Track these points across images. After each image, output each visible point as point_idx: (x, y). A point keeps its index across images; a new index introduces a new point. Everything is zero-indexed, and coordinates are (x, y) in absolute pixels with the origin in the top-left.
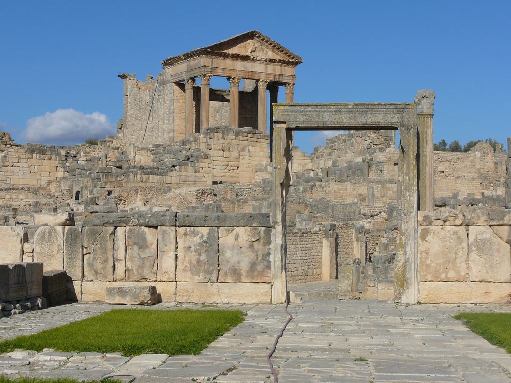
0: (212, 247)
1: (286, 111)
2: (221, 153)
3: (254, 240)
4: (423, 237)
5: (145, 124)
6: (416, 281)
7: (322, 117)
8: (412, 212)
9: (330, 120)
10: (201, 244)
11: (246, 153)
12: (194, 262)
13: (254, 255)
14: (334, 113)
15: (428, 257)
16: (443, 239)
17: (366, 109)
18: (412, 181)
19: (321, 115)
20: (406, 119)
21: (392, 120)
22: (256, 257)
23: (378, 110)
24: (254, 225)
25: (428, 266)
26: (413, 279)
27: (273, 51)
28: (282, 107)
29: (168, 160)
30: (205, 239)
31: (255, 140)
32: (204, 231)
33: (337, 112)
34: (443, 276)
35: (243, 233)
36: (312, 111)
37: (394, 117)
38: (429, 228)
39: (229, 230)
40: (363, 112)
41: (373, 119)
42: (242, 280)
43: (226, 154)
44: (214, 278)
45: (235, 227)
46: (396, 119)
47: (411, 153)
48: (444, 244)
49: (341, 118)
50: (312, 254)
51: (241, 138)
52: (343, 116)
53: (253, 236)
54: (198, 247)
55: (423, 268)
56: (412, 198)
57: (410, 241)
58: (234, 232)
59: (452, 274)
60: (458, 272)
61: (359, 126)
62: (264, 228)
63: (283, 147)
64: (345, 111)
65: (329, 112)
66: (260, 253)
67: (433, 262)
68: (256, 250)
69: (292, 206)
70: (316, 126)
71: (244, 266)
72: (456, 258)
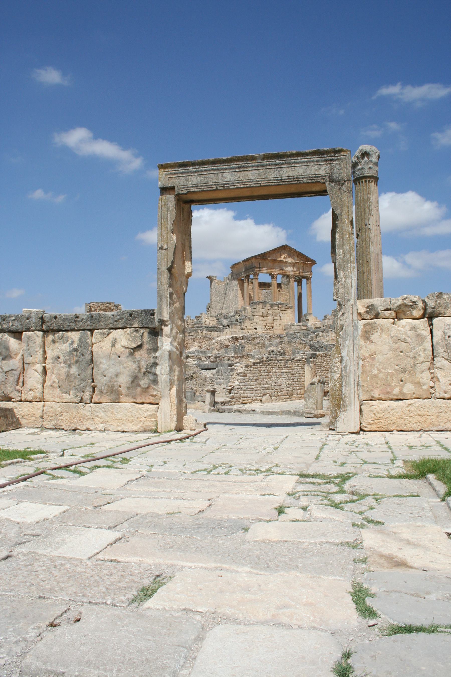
0: (85, 359)
2: (261, 318)
3: (134, 345)
4: (367, 336)
5: (222, 305)
6: (356, 399)
7: (222, 176)
8: (348, 300)
10: (71, 353)
11: (278, 318)
12: (63, 377)
13: (135, 366)
14: (237, 170)
15: (374, 365)
16: (395, 338)
18: (348, 256)
20: (336, 171)
21: (317, 173)
22: (137, 369)
24: (134, 326)
25: (376, 376)
26: (352, 395)
27: (298, 257)
29: (225, 322)
30: (75, 345)
31: (284, 309)
32: (75, 336)
34: (396, 391)
35: (123, 338)
36: (209, 170)
37: (320, 169)
38: (375, 323)
39: (104, 333)
42: (121, 400)
43: (265, 318)
44: (87, 396)
45: (112, 330)
46: (322, 171)
49: (247, 175)
50: (296, 378)
51: (274, 308)
52: (249, 173)
53: (134, 340)
54: (67, 357)
55: (367, 381)
57: (347, 342)
58: (111, 336)
59: (409, 389)
60: (419, 384)
61: (271, 184)
62: (148, 330)
63: (171, 220)
64: (253, 167)
66: (144, 364)
67: (381, 372)
68: (139, 359)
69: (295, 345)
70: (214, 188)
71: (124, 380)
72: (415, 365)
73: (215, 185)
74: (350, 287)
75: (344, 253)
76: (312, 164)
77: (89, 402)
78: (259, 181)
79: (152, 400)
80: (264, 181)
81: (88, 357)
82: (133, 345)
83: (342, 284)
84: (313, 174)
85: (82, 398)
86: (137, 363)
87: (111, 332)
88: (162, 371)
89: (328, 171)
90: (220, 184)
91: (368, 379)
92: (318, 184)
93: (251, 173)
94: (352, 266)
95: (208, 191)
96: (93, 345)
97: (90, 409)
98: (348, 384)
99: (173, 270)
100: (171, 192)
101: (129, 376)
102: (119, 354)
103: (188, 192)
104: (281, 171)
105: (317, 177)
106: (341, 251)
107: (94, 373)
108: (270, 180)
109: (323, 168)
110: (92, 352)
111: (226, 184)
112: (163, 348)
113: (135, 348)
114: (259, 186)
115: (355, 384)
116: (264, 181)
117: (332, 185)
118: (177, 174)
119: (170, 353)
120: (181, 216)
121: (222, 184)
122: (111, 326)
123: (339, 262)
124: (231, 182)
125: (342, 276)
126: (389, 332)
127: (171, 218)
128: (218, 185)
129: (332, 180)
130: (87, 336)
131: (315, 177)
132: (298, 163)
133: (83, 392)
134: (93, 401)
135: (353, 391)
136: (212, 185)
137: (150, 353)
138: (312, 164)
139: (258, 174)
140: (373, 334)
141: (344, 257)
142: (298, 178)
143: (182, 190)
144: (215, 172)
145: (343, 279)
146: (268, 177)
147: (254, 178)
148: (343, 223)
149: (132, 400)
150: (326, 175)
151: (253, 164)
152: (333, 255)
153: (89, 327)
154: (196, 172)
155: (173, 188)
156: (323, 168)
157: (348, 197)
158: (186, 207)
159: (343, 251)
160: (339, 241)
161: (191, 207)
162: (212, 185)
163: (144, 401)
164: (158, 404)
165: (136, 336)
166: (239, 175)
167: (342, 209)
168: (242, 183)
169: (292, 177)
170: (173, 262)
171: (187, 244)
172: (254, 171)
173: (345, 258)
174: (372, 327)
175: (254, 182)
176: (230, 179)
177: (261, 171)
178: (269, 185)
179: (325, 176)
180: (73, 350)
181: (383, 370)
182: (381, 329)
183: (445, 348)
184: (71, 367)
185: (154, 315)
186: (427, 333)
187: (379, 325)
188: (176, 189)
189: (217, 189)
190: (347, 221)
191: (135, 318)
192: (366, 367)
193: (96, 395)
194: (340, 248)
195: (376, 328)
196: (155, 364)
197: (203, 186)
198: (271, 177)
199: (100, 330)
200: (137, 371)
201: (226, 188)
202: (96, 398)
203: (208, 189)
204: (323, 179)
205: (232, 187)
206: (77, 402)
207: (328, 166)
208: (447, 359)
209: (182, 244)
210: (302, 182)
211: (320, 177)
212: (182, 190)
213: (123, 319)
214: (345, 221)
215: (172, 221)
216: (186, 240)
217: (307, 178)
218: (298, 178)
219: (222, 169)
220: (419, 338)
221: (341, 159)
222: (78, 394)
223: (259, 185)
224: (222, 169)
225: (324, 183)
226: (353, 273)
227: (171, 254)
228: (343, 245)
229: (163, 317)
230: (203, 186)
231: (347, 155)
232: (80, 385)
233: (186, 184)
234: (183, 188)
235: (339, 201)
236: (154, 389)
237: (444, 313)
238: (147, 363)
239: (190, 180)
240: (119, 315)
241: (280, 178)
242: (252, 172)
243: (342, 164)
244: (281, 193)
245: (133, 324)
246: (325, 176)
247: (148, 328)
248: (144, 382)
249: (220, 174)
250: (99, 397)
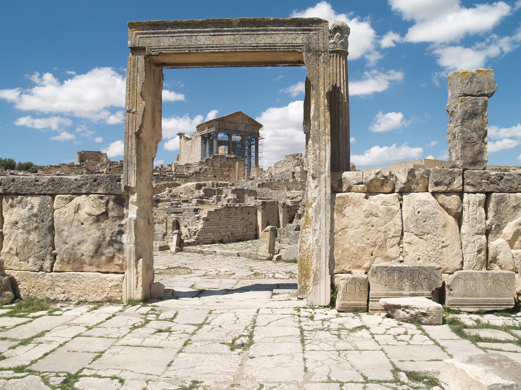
3: (98, 213)
6: (328, 273)
7: (196, 39)
8: (322, 173)
14: (212, 34)
18: (323, 128)
20: (313, 41)
21: (294, 42)
22: (102, 237)
24: (99, 192)
36: (182, 32)
37: (297, 38)
42: (84, 269)
44: (47, 264)
45: (74, 196)
47: (322, 88)
48: (369, 219)
49: (222, 40)
52: (224, 37)
53: (99, 206)
54: (26, 223)
56: (323, 153)
57: (320, 216)
58: (74, 201)
62: (113, 197)
63: (140, 83)
67: (353, 246)
68: (103, 227)
71: (87, 248)
73: (188, 48)
74: (324, 159)
77: (49, 270)
78: (234, 47)
79: (117, 269)
80: (240, 46)
81: (47, 223)
82: (97, 213)
85: (42, 266)
86: (101, 231)
87: (74, 198)
88: (128, 240)
89: (305, 41)
90: (193, 48)
91: (340, 253)
92: (294, 54)
95: (181, 53)
96: (54, 211)
97: (50, 278)
98: (319, 257)
99: (141, 134)
100: (142, 53)
101: (93, 244)
102: (82, 221)
103: (160, 53)
105: (295, 46)
106: (316, 122)
107: (55, 240)
108: (246, 46)
109: (301, 37)
110: (53, 218)
111: (199, 48)
112: (129, 216)
113: (99, 215)
114: (234, 52)
115: (326, 257)
116: (240, 46)
119: (136, 222)
120: (152, 79)
121: (195, 48)
122: (73, 191)
123: (314, 134)
124: (205, 46)
125: (316, 148)
126: (361, 206)
127: (140, 80)
128: (191, 48)
129: (309, 50)
130: (48, 201)
131: (292, 46)
132: (276, 30)
133: (43, 260)
134: (53, 270)
135: (324, 265)
136: (184, 48)
137: (115, 221)
139: (234, 39)
140: (345, 208)
142: (275, 46)
143: (153, 52)
144: (189, 34)
146: (244, 43)
147: (230, 43)
149: (96, 270)
152: (305, 126)
153: (50, 192)
155: (143, 49)
158: (157, 69)
160: (315, 112)
161: (162, 70)
162: (184, 48)
163: (109, 270)
164: (124, 273)
165: (100, 203)
168: (217, 47)
170: (141, 126)
171: (157, 108)
172: (229, 36)
173: (320, 130)
174: (345, 201)
175: (229, 47)
177: (237, 36)
178: (244, 51)
179: (302, 46)
180: (32, 215)
181: (354, 244)
182: (353, 203)
183: (415, 223)
184: (31, 234)
185: (120, 181)
186: (396, 208)
187: (351, 199)
188: (146, 50)
189: (189, 53)
190: (322, 93)
191: (99, 184)
192: (337, 240)
193: (57, 263)
194: (314, 119)
195: (349, 201)
196: (121, 233)
197: (175, 48)
198: (246, 43)
199: (61, 195)
200: (101, 240)
202: (56, 267)
203: (181, 52)
204: (300, 49)
205: (206, 51)
206: (36, 270)
207: (306, 35)
208: (416, 235)
209: (152, 107)
211: (297, 46)
212: (153, 52)
213: (87, 184)
215: (142, 83)
216: (156, 104)
217: (283, 46)
218: (275, 46)
220: (390, 213)
221: (319, 29)
222: (38, 262)
223: (234, 50)
225: (301, 53)
227: (139, 117)
229: (130, 184)
230: (175, 48)
231: (325, 26)
232: (40, 252)
233: (158, 45)
234: (154, 49)
236: (119, 259)
237: (414, 188)
238: (112, 231)
239: (161, 41)
240: (83, 180)
242: (227, 37)
244: (255, 61)
245: (97, 190)
247: (114, 194)
248: (108, 251)
249: (194, 37)
250: (61, 265)
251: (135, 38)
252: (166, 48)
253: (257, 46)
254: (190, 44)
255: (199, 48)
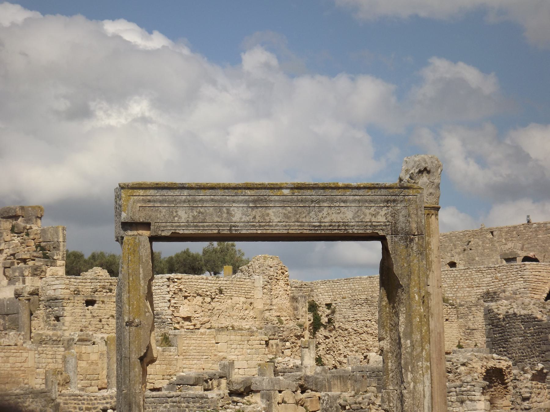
1: (149, 201)
7: (228, 213)
9: (245, 219)
14: (251, 205)
17: (321, 197)
18: (419, 350)
19: (224, 209)
20: (402, 219)
21: (373, 219)
23: (344, 198)
28: (141, 192)
33: (257, 203)
36: (207, 201)
37: (378, 213)
40: (312, 201)
41: (336, 217)
46: (381, 219)
49: (268, 215)
52: (271, 211)
56: (420, 387)
61: (305, 232)
63: (144, 279)
64: (275, 201)
65: (241, 202)
70: (216, 232)
73: (216, 226)
74: (422, 396)
75: (413, 346)
76: (367, 205)
83: (409, 392)
84: (368, 220)
90: (224, 226)
93: (273, 212)
94: (424, 366)
104: (320, 212)
105: (375, 226)
106: (409, 341)
109: (383, 212)
111: (234, 226)
116: (294, 226)
117: (396, 240)
118: (154, 201)
121: (227, 226)
123: (407, 358)
124: (242, 224)
125: (409, 380)
128: (221, 226)
129: (395, 233)
132: (344, 202)
138: (367, 205)
139: (285, 214)
141: (412, 351)
142: (345, 226)
145: (412, 384)
146: (300, 220)
147: (279, 220)
148: (410, 298)
150: (388, 224)
151: (277, 198)
154: (184, 202)
156: (383, 212)
157: (418, 261)
159: (412, 342)
160: (406, 326)
162: (211, 226)
166: (254, 213)
167: (410, 278)
168: (260, 226)
169: (337, 224)
173: (415, 353)
176: (241, 218)
179: (386, 225)
188: (152, 227)
194: (406, 339)
197: (196, 226)
198: (304, 220)
201: (234, 232)
205: (244, 232)
207: (390, 209)
210: (350, 231)
214: (415, 297)
217: (358, 226)
218: (345, 226)
219: (228, 201)
221: (409, 200)
223: (285, 232)
224: (228, 201)
226: (425, 376)
228: (411, 333)
231: (419, 195)
235: (405, 265)
239: (175, 214)
241: (318, 224)
242: (274, 210)
243: (411, 208)
246: (386, 225)
251: (132, 208)
252: (183, 226)
253: (320, 226)
254: (219, 220)
255: (234, 226)
